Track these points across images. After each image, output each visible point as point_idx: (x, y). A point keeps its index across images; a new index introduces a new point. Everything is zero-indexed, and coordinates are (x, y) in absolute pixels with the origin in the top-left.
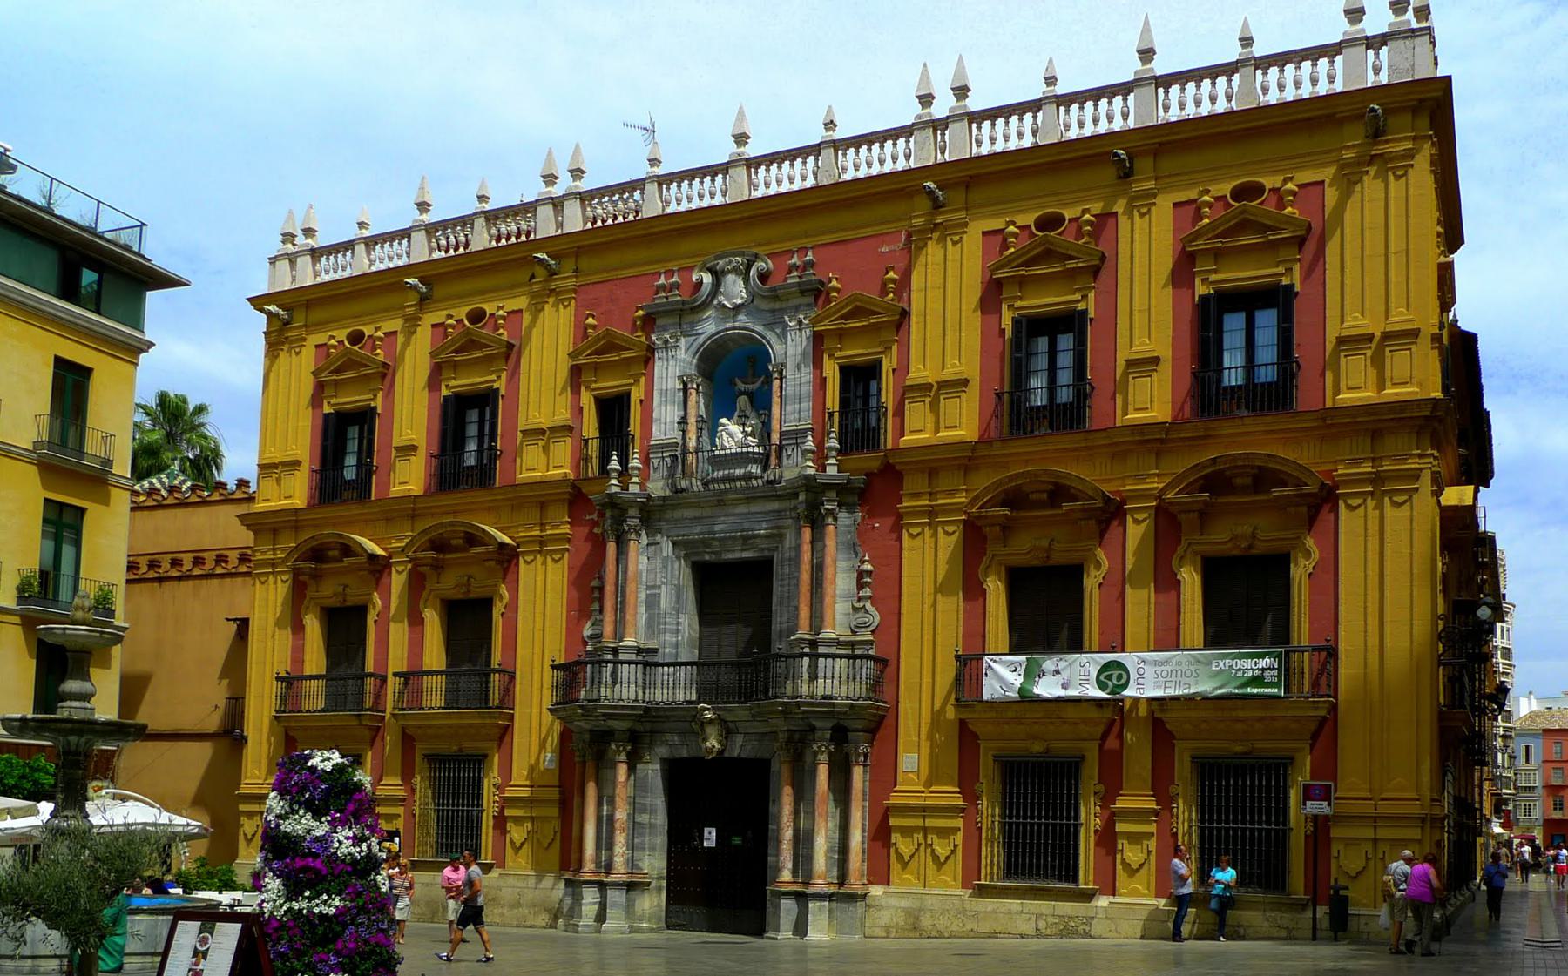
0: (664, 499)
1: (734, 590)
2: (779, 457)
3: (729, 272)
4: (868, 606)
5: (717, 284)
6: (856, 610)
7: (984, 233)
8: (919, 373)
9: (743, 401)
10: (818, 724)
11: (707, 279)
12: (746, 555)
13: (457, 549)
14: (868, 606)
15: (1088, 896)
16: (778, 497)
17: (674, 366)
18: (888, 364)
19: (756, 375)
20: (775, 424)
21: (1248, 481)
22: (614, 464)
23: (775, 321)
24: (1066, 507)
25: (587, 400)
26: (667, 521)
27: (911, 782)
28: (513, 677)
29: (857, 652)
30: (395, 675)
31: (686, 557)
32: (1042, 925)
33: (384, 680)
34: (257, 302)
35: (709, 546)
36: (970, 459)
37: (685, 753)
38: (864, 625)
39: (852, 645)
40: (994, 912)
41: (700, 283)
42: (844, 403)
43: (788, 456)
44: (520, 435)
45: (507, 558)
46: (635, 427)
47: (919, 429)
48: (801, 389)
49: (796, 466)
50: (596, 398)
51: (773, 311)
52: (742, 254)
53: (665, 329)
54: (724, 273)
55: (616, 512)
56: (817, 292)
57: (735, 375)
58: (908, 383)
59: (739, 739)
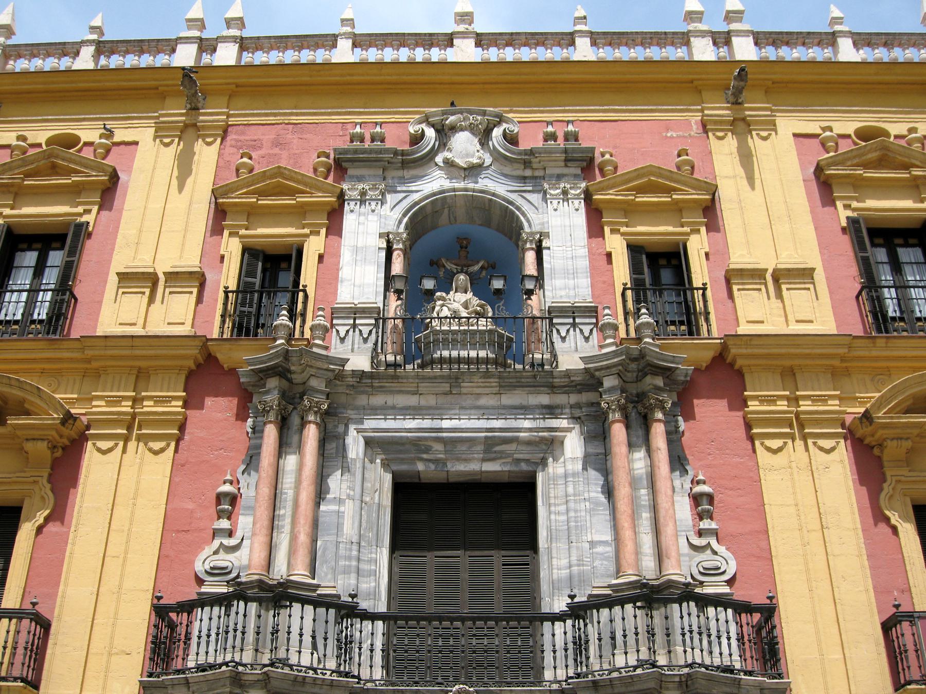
3: (462, 130)
4: (714, 543)
7: (795, 135)
11: (430, 133)
12: (489, 467)
25: (232, 248)
26: (356, 408)
28: (45, 625)
31: (385, 465)
35: (428, 450)
36: (843, 359)
38: (715, 571)
41: (417, 139)
43: (563, 339)
44: (113, 280)
50: (246, 250)
53: (360, 179)
54: (454, 129)
56: (585, 163)
58: (732, 266)
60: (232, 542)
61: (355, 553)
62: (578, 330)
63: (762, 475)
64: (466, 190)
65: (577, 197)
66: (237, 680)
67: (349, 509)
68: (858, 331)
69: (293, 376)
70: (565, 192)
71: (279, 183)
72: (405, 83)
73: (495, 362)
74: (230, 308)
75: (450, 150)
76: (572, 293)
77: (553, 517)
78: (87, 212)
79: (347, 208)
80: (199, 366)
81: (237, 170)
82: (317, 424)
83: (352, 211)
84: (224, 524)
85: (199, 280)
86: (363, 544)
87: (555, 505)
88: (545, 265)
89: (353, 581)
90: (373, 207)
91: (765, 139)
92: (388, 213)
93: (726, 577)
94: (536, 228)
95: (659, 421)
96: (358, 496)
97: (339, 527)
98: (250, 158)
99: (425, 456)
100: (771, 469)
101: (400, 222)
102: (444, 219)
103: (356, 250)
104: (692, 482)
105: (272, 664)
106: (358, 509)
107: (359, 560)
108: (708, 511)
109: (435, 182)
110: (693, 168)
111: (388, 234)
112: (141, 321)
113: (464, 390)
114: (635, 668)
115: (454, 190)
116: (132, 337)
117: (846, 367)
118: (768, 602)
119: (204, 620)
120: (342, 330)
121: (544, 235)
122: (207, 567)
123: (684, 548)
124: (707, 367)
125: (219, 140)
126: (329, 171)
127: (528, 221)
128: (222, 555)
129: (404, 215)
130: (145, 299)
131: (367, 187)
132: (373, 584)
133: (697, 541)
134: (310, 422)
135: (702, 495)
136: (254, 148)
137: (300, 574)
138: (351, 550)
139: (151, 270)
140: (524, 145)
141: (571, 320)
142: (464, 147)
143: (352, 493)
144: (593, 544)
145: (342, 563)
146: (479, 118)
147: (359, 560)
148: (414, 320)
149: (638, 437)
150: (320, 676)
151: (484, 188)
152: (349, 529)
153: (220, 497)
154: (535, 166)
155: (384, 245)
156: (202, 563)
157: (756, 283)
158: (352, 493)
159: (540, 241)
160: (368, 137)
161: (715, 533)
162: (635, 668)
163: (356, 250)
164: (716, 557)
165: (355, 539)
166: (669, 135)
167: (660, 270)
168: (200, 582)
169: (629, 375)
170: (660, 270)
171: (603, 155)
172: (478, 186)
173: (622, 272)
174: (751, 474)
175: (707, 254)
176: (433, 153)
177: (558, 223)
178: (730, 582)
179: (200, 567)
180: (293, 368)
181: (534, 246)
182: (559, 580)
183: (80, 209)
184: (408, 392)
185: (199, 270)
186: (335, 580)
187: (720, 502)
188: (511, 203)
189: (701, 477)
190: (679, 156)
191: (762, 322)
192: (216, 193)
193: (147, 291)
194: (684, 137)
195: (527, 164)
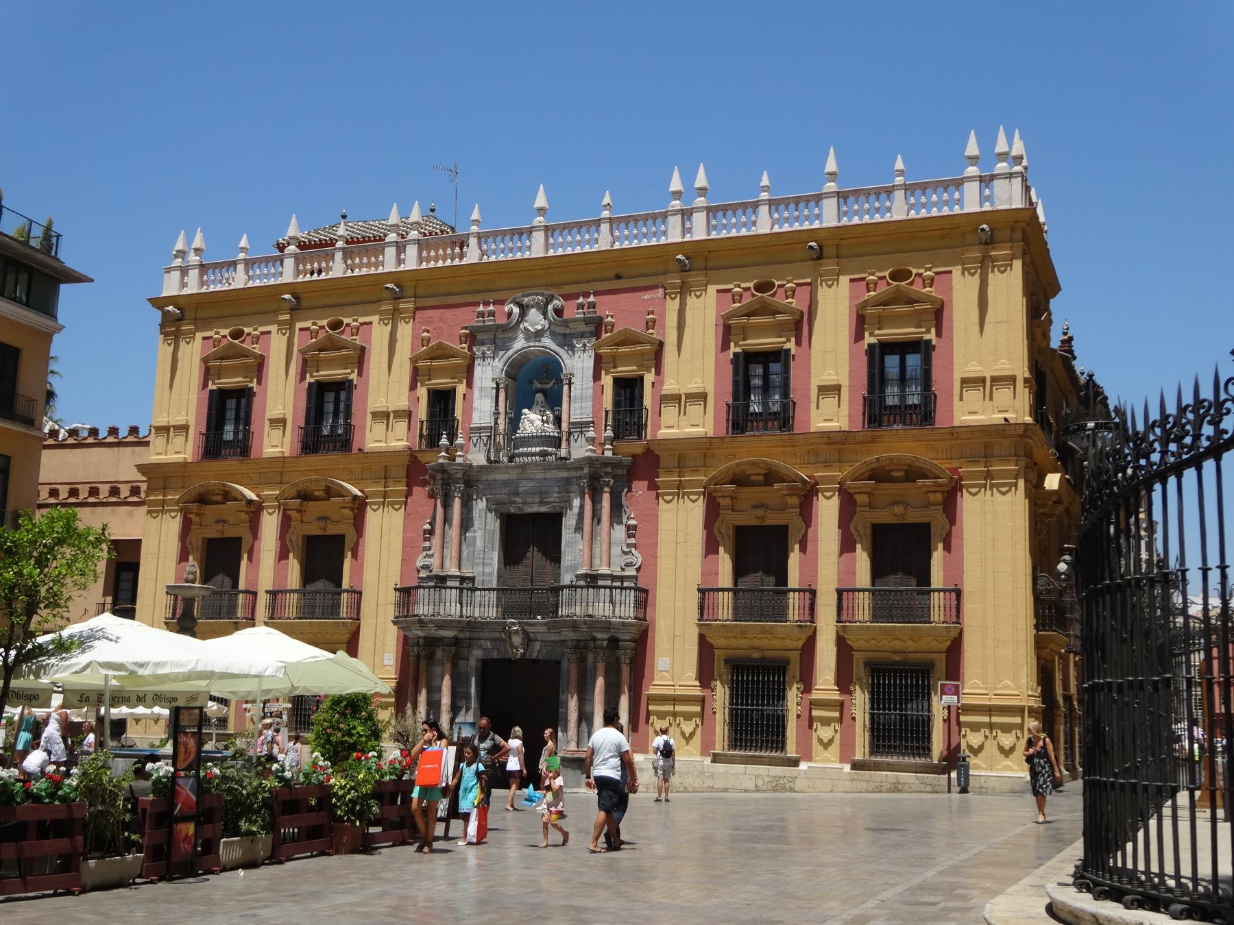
0: (481, 467)
1: (530, 536)
2: (568, 440)
3: (533, 307)
5: (523, 314)
6: (625, 553)
8: (670, 387)
9: (539, 397)
10: (599, 636)
11: (516, 310)
12: (543, 509)
13: (317, 499)
15: (794, 763)
17: (488, 373)
18: (649, 378)
19: (549, 379)
20: (564, 417)
21: (901, 474)
22: (444, 441)
23: (566, 341)
24: (776, 486)
25: (422, 392)
27: (664, 678)
28: (360, 593)
29: (626, 584)
30: (267, 592)
32: (760, 782)
33: (255, 594)
34: (159, 303)
37: (495, 655)
39: (622, 578)
40: (726, 773)
41: (510, 314)
42: (616, 403)
44: (369, 417)
45: (359, 507)
46: (458, 413)
47: (671, 426)
48: (586, 391)
49: (580, 450)
50: (429, 391)
51: (564, 335)
52: (542, 295)
53: (483, 344)
54: (528, 307)
56: (597, 326)
57: (535, 382)
58: (663, 392)
59: (537, 646)
60: (430, 553)
66: (421, 622)
67: (479, 534)
68: (723, 433)
70: (584, 346)
74: (425, 432)
84: (427, 544)
85: (408, 414)
97: (474, 543)
103: (481, 389)
109: (520, 343)
123: (620, 553)
133: (625, 549)
137: (454, 571)
152: (479, 544)
153: (425, 531)
156: (420, 562)
161: (635, 546)
163: (481, 389)
168: (418, 571)
176: (518, 323)
179: (419, 564)
192: (414, 360)
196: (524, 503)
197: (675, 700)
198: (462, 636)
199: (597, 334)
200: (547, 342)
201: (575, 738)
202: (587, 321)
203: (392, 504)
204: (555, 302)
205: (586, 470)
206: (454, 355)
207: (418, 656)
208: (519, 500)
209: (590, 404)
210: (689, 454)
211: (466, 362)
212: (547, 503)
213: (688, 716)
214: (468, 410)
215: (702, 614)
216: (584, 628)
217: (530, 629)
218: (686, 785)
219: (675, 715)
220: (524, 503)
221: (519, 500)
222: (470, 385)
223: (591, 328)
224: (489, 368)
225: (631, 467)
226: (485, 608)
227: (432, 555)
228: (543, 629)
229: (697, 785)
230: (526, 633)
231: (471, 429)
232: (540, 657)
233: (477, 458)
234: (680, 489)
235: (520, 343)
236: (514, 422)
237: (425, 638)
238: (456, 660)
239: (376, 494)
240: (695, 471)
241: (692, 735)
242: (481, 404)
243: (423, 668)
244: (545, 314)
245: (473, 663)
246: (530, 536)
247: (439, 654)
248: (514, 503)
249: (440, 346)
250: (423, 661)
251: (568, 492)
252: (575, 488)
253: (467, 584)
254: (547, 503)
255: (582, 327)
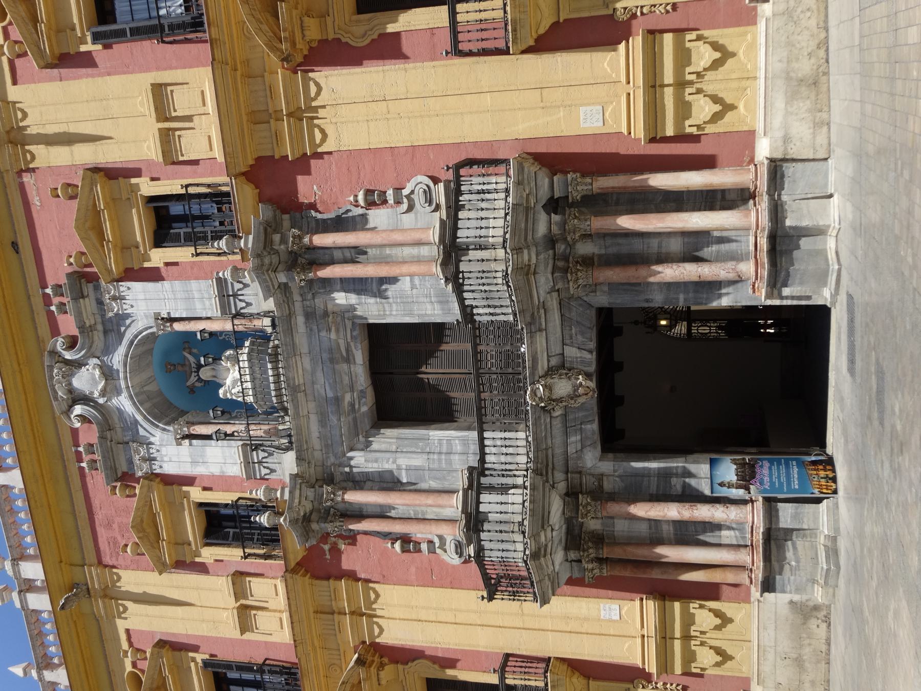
0: (300, 459)
1: (405, 377)
3: (70, 384)
4: (405, 192)
5: (85, 399)
6: (411, 208)
11: (78, 409)
14: (405, 192)
16: (291, 315)
17: (171, 454)
18: (148, 188)
22: (264, 519)
23: (113, 327)
25: (208, 554)
28: (507, 656)
37: (593, 427)
38: (428, 194)
43: (249, 304)
44: (248, 636)
48: (177, 294)
51: (106, 332)
52: (51, 368)
53: (130, 462)
54: (71, 390)
55: (314, 516)
56: (83, 280)
58: (161, 159)
59: (571, 352)
60: (436, 540)
61: (436, 457)
62: (239, 293)
63: (345, 149)
64: (126, 378)
65: (117, 288)
66: (535, 556)
67: (404, 461)
68: (204, 50)
69: (308, 511)
70: (114, 298)
71: (147, 529)
72: (33, 430)
73: (275, 362)
75: (92, 393)
76: (207, 303)
77: (394, 313)
78: (194, 660)
79: (158, 471)
80: (307, 571)
81: (138, 554)
82: (343, 494)
83: (161, 467)
84: (424, 547)
85: (239, 577)
86: (428, 450)
87: (384, 311)
88: (184, 316)
89: (457, 457)
90: (154, 451)
91: (25, 115)
92: (157, 438)
93: (431, 184)
94: (152, 322)
95: (311, 240)
96: (394, 455)
97: (417, 469)
98: (126, 546)
99: (357, 406)
100: (338, 139)
101: (164, 430)
102: (152, 388)
103: (194, 463)
104: (357, 206)
105: (523, 533)
106: (403, 455)
107: (440, 453)
108: (379, 195)
109: (124, 403)
110: (69, 185)
111: (176, 439)
112: (278, 615)
113: (301, 381)
114: (509, 286)
115: (128, 387)
116: (292, 623)
117: (241, 63)
118: (451, 170)
119: (493, 554)
120: (264, 471)
121: (157, 317)
122: (456, 557)
123: (411, 215)
124: (257, 187)
125: (115, 570)
126: (128, 486)
127: (146, 329)
128: (447, 547)
129: (157, 426)
130: (260, 613)
131: (137, 457)
132: (457, 442)
133: (405, 206)
134: (343, 499)
135: (366, 200)
136: (115, 542)
137: (456, 501)
138: (434, 459)
139: (235, 611)
140: (75, 332)
141: (231, 298)
142: (87, 380)
143: (391, 460)
144: (413, 287)
145: (444, 466)
146: (56, 371)
147: (440, 453)
148: (247, 411)
149: (325, 254)
150: (528, 497)
151: (122, 364)
152: (418, 461)
153: (404, 550)
154: (93, 322)
155: (187, 441)
157: (174, 139)
158: (391, 460)
159: (163, 319)
160: (91, 457)
161: (398, 190)
162: (509, 286)
163: (194, 463)
164: (416, 192)
165: (425, 456)
166: (38, 204)
167: (171, 220)
169: (274, 261)
170: (171, 220)
171: (71, 264)
172: (121, 370)
173: (182, 254)
174: (345, 156)
175: (153, 179)
177: (142, 304)
178: (436, 180)
179: (456, 560)
180: (302, 514)
181: (168, 324)
182: (443, 309)
183: (192, 664)
184: (308, 422)
185: (229, 578)
186: (456, 471)
187: (371, 184)
188: (132, 342)
189: (352, 199)
190: (58, 196)
191: (209, 137)
192: (162, 568)
193: (253, 612)
194: (38, 189)
195: (92, 328)
196: (352, 389)
197: (653, 86)
198: (562, 486)
199: (92, 279)
200: (117, 359)
201: (730, 265)
202: (79, 295)
203: (369, 604)
204: (59, 349)
205: (282, 278)
206: (147, 504)
207: (600, 560)
208: (348, 398)
209: (194, 284)
210: (245, 110)
211: (157, 486)
212: (348, 350)
213: (683, 57)
214: (225, 482)
215: (498, 52)
216: (529, 256)
217: (543, 366)
218: (813, 44)
219: (681, 84)
220: (352, 389)
221: (348, 398)
222: (190, 481)
223: (89, 289)
224: (164, 451)
225: (273, 204)
226: (511, 448)
227: (441, 538)
228: (540, 340)
229: (813, 23)
230: (551, 372)
231: (249, 477)
232: (592, 345)
233: (287, 464)
234: (303, 114)
235: (124, 403)
236: (231, 409)
237: (567, 549)
238: (600, 495)
239: (356, 628)
240: (271, 91)
241: (716, 46)
242: (211, 463)
243: (617, 553)
244: (78, 365)
245: (607, 466)
246: (405, 377)
247: (593, 525)
248: (352, 405)
249: (138, 526)
250: (605, 553)
251: (326, 314)
252: (319, 302)
253: (478, 478)
254: (348, 350)
255: (88, 304)
